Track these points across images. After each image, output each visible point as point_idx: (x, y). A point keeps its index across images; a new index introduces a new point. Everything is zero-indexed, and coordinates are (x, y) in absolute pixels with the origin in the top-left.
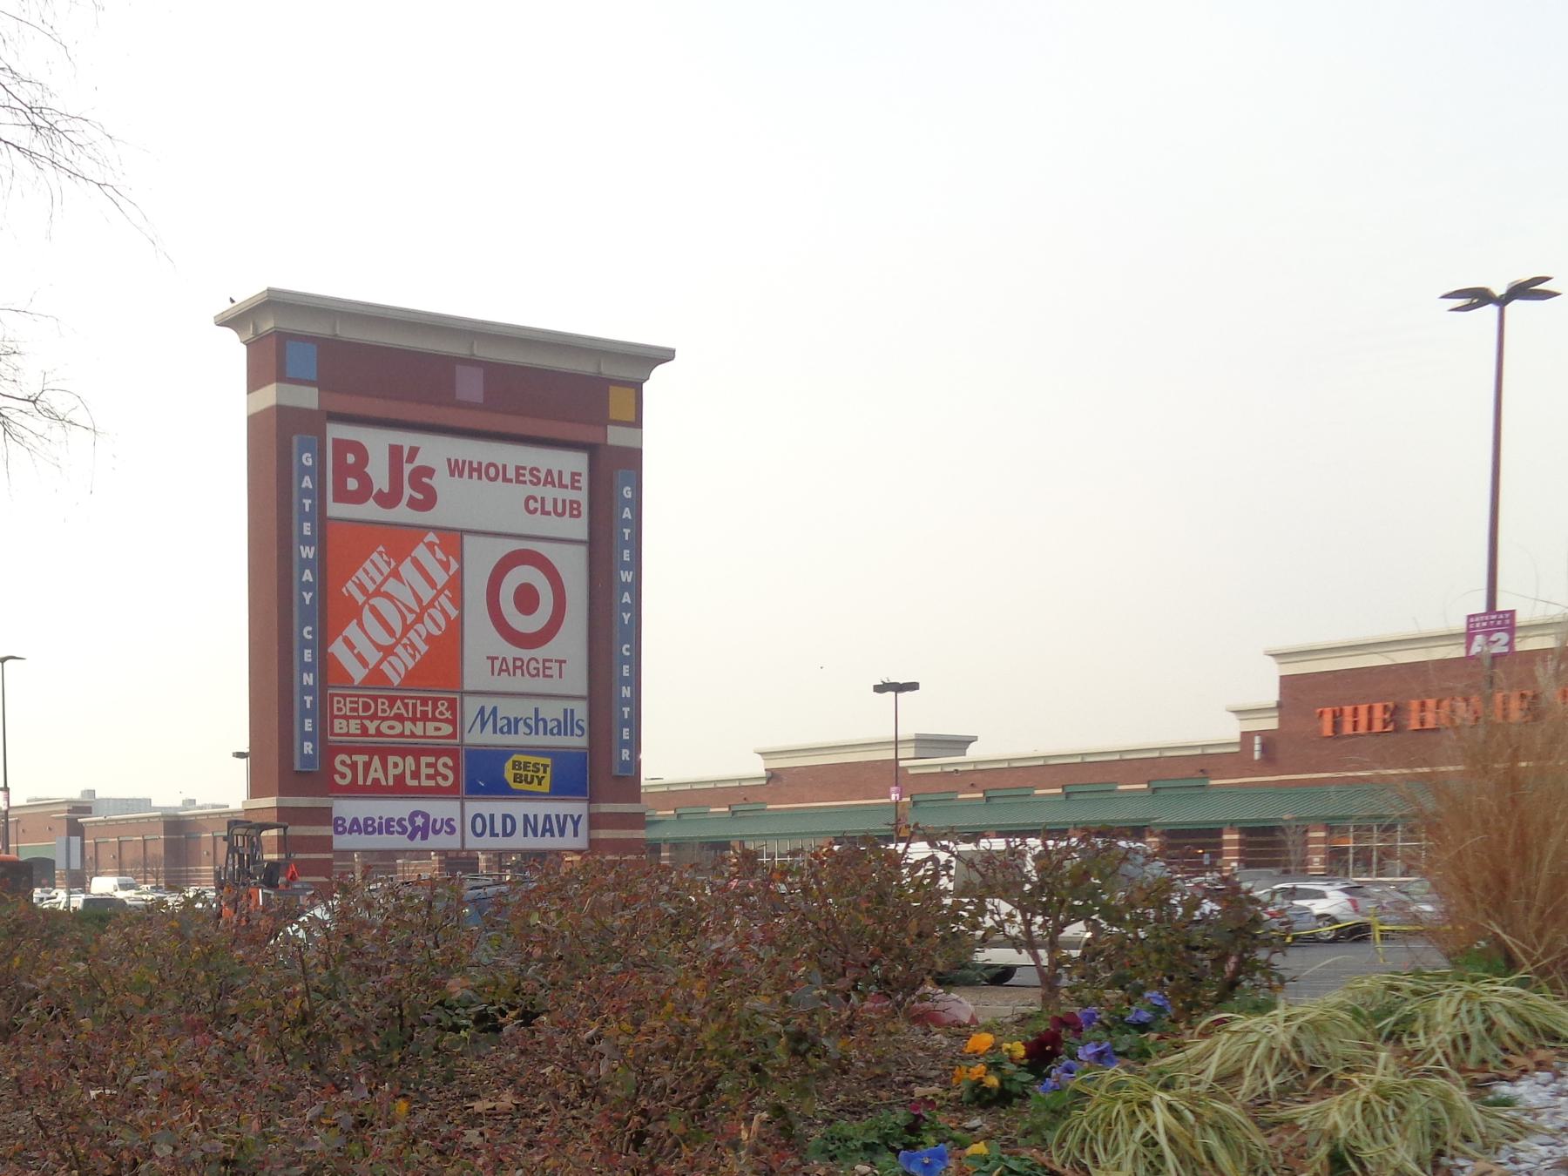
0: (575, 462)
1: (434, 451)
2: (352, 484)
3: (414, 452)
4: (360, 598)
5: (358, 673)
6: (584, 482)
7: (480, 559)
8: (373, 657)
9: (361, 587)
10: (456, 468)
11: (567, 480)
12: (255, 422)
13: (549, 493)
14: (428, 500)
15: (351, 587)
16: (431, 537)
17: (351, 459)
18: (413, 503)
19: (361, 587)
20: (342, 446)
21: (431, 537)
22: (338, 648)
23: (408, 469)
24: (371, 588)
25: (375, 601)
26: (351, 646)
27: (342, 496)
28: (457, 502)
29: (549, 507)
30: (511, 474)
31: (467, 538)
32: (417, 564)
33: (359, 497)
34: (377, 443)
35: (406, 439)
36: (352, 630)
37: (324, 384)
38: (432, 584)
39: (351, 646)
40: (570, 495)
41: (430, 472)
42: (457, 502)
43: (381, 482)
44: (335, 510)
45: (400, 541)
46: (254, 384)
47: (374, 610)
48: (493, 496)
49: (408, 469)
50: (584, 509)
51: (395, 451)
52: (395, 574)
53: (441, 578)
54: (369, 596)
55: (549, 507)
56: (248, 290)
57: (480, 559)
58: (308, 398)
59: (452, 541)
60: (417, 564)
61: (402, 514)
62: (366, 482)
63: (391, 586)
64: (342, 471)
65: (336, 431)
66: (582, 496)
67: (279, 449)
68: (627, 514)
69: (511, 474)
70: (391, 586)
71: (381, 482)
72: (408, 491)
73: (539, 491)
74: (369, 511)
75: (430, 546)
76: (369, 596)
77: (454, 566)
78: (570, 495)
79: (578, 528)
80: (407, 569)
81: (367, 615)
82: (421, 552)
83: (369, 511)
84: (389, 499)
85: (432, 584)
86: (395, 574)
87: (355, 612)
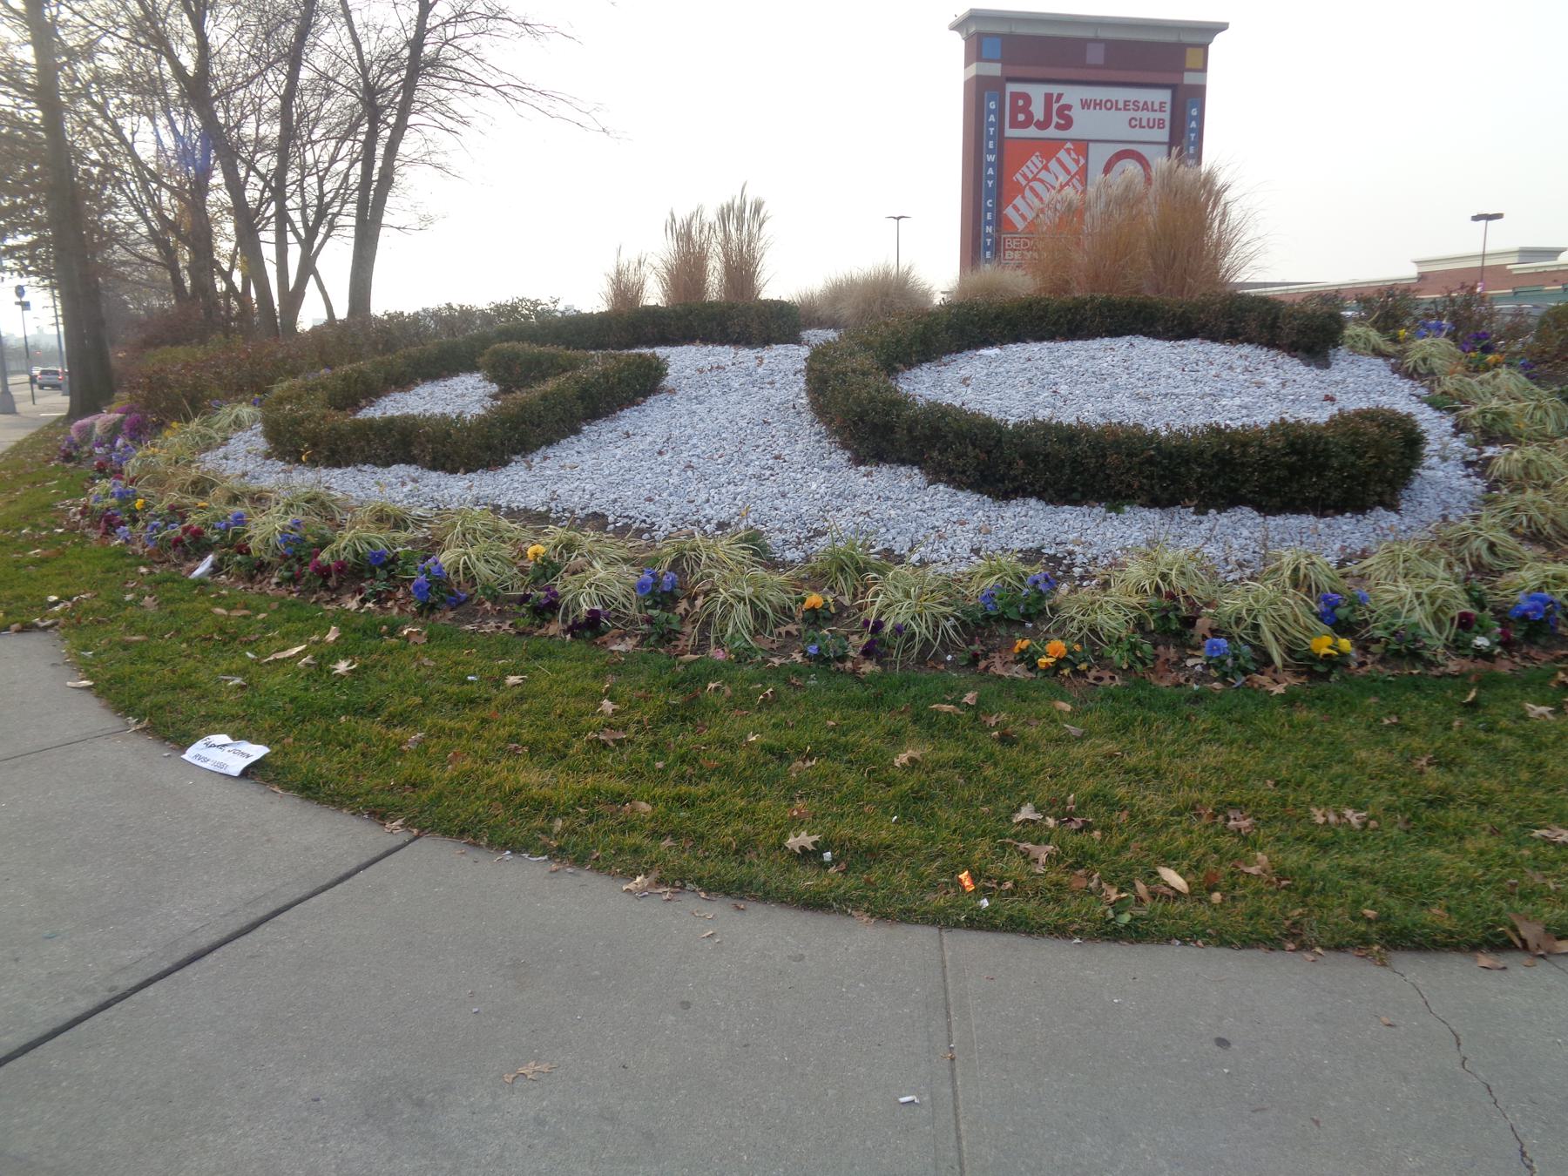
0: (1164, 96)
1: (1072, 95)
2: (1021, 117)
3: (1060, 96)
4: (1024, 182)
5: (1020, 225)
6: (1168, 107)
7: (1099, 155)
8: (1030, 215)
9: (1025, 176)
10: (1085, 104)
11: (1157, 106)
12: (967, 84)
13: (1145, 115)
14: (1068, 123)
15: (1018, 176)
16: (1069, 145)
17: (1021, 103)
18: (1058, 126)
19: (1025, 176)
20: (1015, 96)
21: (1069, 145)
22: (1009, 211)
23: (1055, 106)
24: (1031, 176)
25: (1036, 184)
26: (1016, 208)
27: (1015, 124)
28: (1085, 124)
29: (1144, 123)
30: (1121, 105)
31: (1091, 145)
32: (1059, 161)
33: (1028, 122)
34: (1037, 93)
35: (1055, 89)
36: (1018, 201)
37: (1004, 61)
38: (1068, 172)
39: (1016, 208)
40: (1158, 115)
41: (1069, 107)
42: (1085, 124)
43: (1039, 114)
44: (1010, 132)
45: (1049, 149)
46: (967, 65)
47: (1032, 189)
48: (1105, 117)
49: (1055, 106)
50: (1167, 124)
51: (1048, 97)
52: (1046, 168)
53: (1073, 168)
54: (1029, 181)
55: (1144, 123)
56: (962, 11)
57: (1099, 155)
58: (995, 69)
59: (1082, 146)
60: (1059, 161)
61: (1052, 132)
62: (1030, 116)
63: (1043, 175)
64: (1015, 110)
65: (1012, 88)
66: (1166, 116)
67: (983, 100)
68: (1193, 125)
69: (1121, 105)
70: (1043, 175)
71: (1039, 114)
72: (1055, 119)
73: (1138, 114)
74: (1032, 132)
75: (1068, 151)
76: (1029, 181)
77: (1082, 161)
78: (1158, 115)
79: (1163, 135)
80: (1053, 164)
81: (1028, 193)
82: (1062, 154)
83: (1032, 132)
84: (1043, 125)
85: (1068, 172)
86: (1046, 168)
87: (1021, 190)
